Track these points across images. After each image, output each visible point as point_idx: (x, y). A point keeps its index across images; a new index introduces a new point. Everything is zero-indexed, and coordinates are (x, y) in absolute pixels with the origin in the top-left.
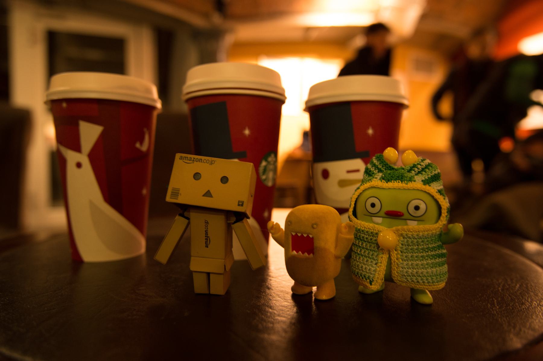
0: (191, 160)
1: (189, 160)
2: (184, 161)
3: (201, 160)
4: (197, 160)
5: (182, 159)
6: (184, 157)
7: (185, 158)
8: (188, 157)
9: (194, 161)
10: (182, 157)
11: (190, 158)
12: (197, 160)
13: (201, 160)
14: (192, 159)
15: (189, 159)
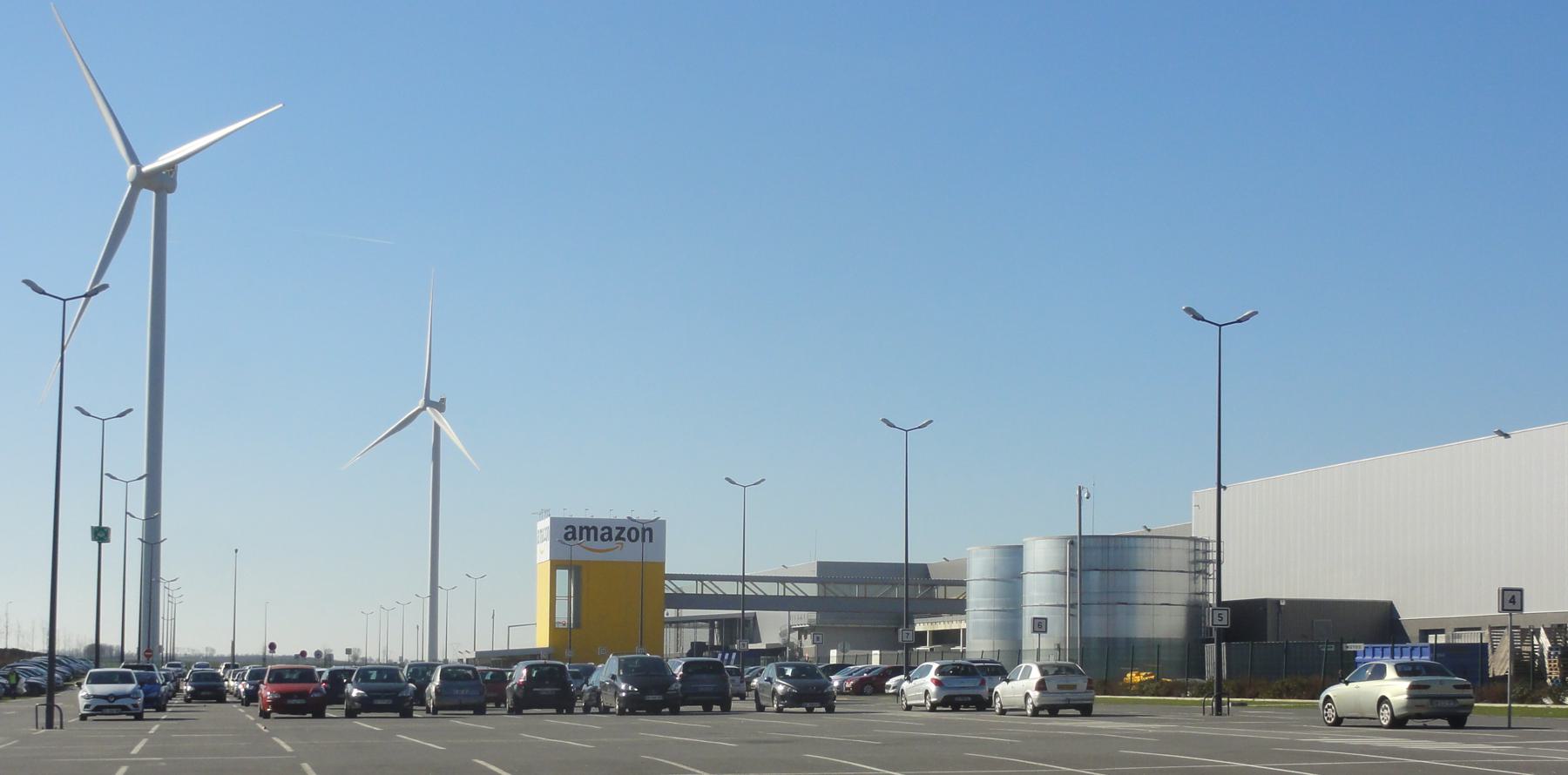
0: (610, 538)
1: (603, 539)
2: (588, 544)
3: (647, 533)
4: (633, 532)
5: (574, 537)
6: (581, 528)
7: (585, 531)
8: (595, 528)
9: (624, 539)
10: (573, 527)
11: (603, 529)
12: (633, 532)
13: (647, 533)
14: (615, 533)
15: (600, 533)
